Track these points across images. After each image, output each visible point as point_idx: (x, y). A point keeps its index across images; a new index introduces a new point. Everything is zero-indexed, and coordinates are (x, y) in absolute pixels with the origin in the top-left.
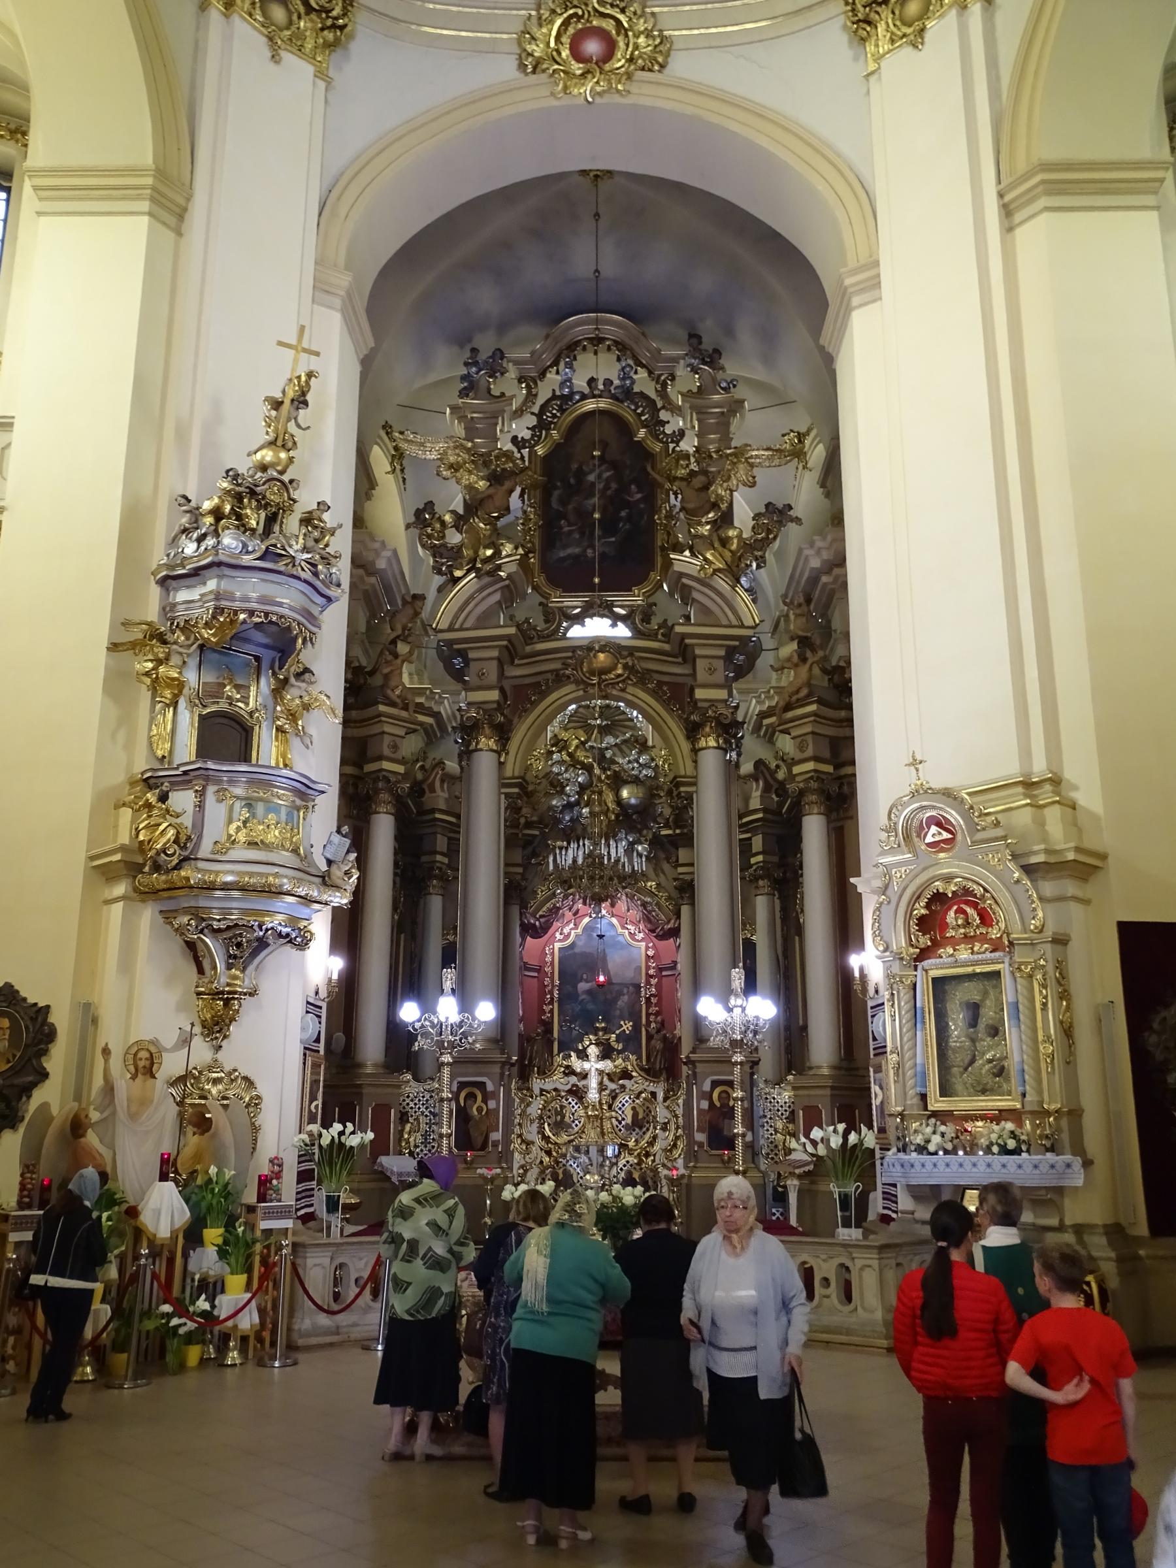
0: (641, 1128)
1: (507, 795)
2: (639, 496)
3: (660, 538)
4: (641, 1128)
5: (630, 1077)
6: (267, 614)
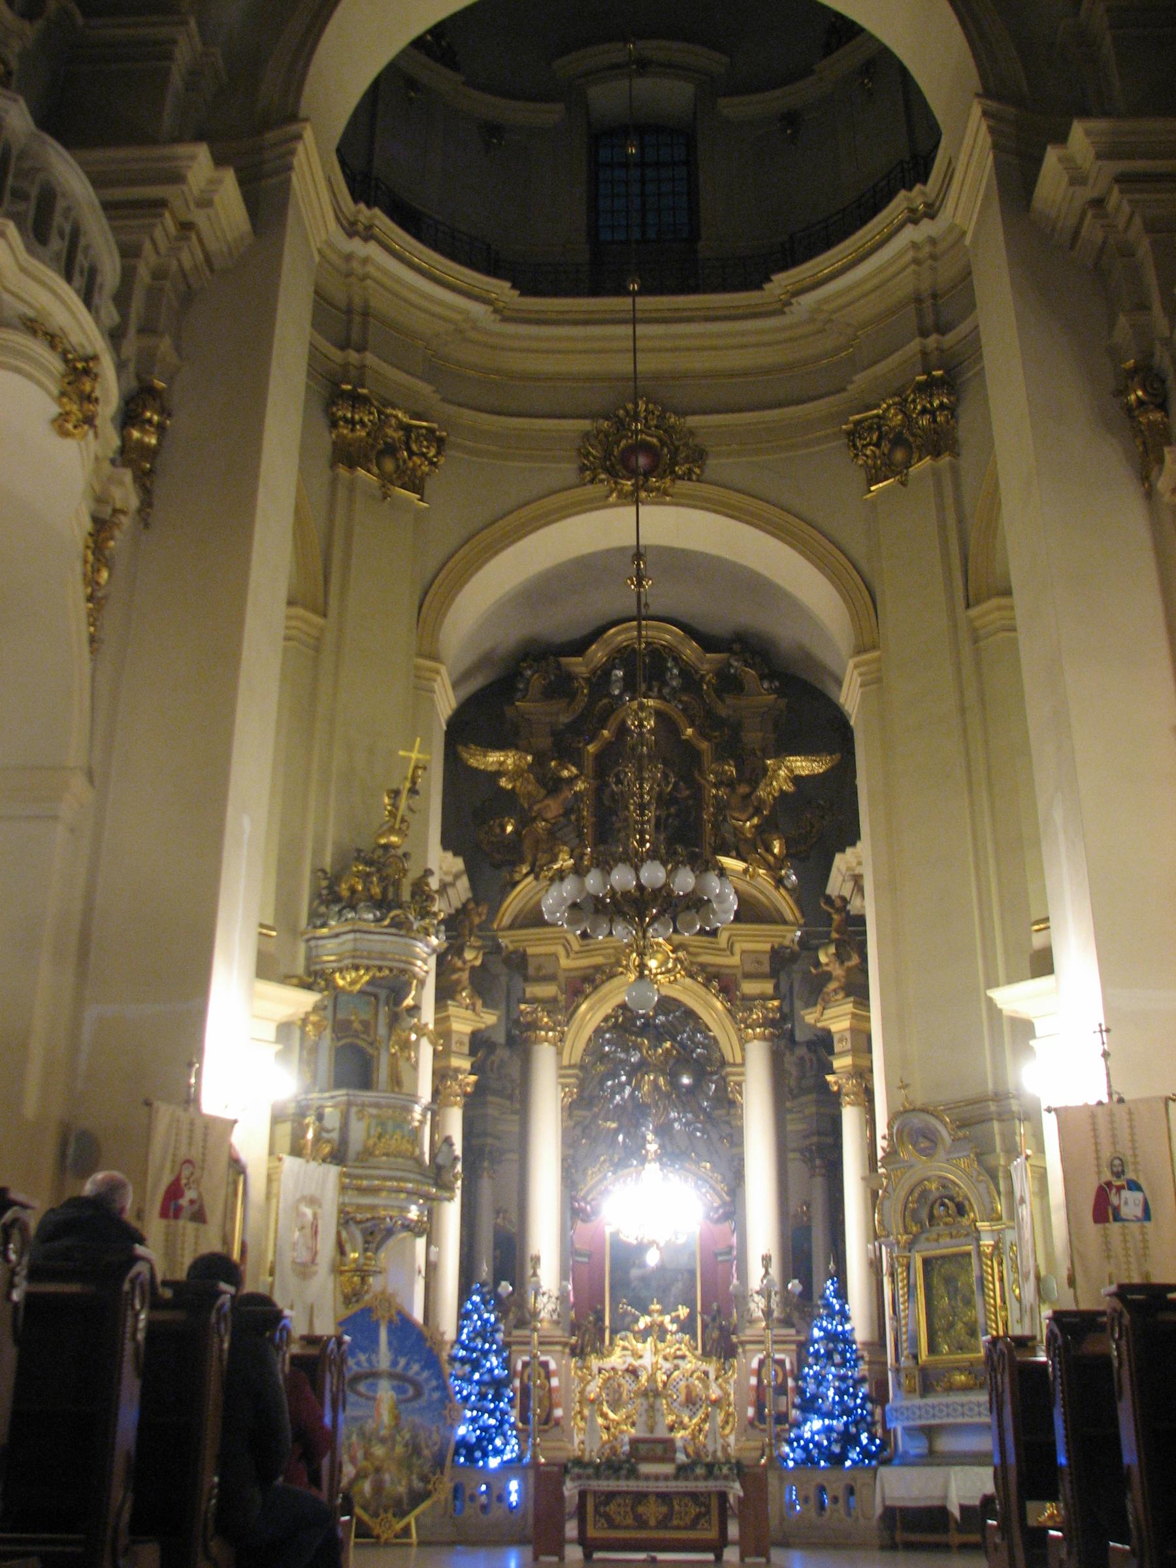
0: (694, 1404)
1: (564, 1086)
2: (688, 792)
3: (709, 838)
4: (694, 1404)
5: (683, 1357)
6: (391, 970)
